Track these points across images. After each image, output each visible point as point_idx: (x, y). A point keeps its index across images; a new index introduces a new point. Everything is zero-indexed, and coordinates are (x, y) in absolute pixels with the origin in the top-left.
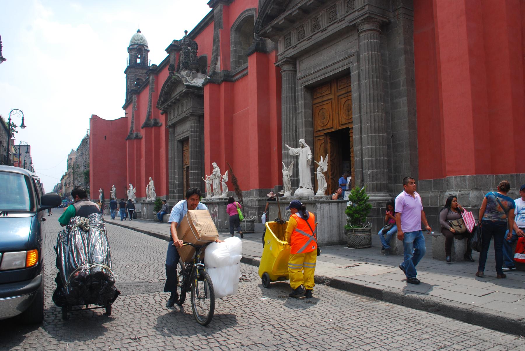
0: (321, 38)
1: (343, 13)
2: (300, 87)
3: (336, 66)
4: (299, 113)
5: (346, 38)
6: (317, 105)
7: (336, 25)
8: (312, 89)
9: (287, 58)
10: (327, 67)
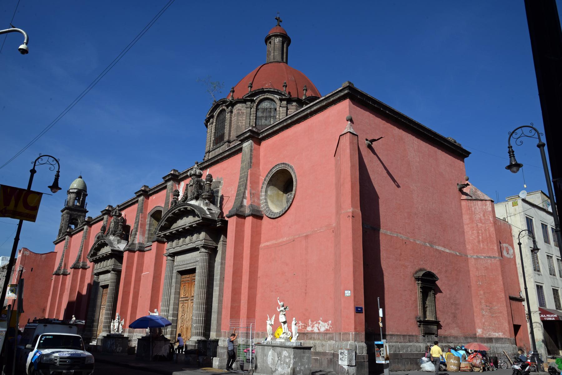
2: (175, 271)
3: (191, 265)
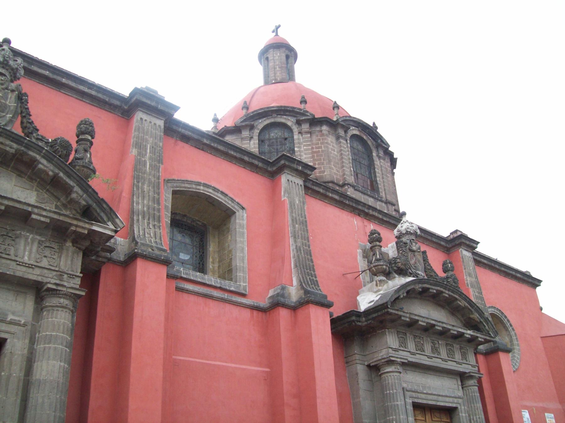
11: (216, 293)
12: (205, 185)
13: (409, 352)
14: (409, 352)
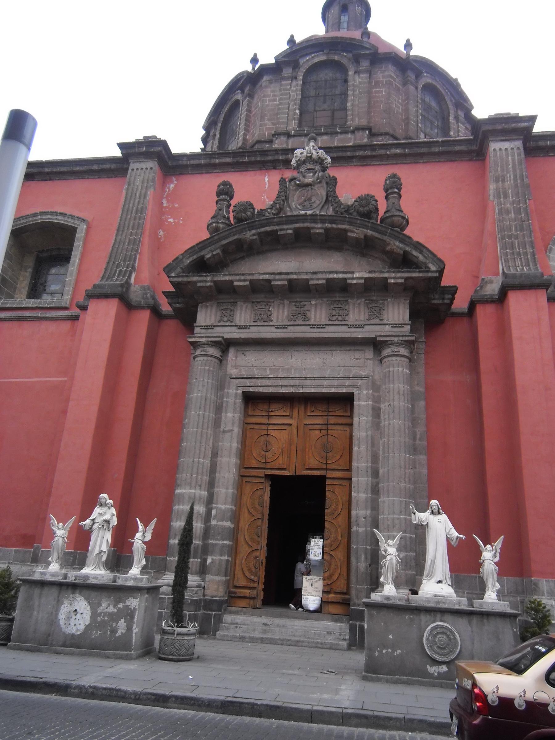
0: (308, 336)
1: (362, 318)
3: (325, 383)
4: (224, 432)
5: (349, 350)
6: (252, 426)
7: (344, 328)
8: (251, 400)
9: (223, 337)
10: (306, 379)
11: (28, 314)
12: (42, 214)
13: (236, 326)
14: (236, 326)
